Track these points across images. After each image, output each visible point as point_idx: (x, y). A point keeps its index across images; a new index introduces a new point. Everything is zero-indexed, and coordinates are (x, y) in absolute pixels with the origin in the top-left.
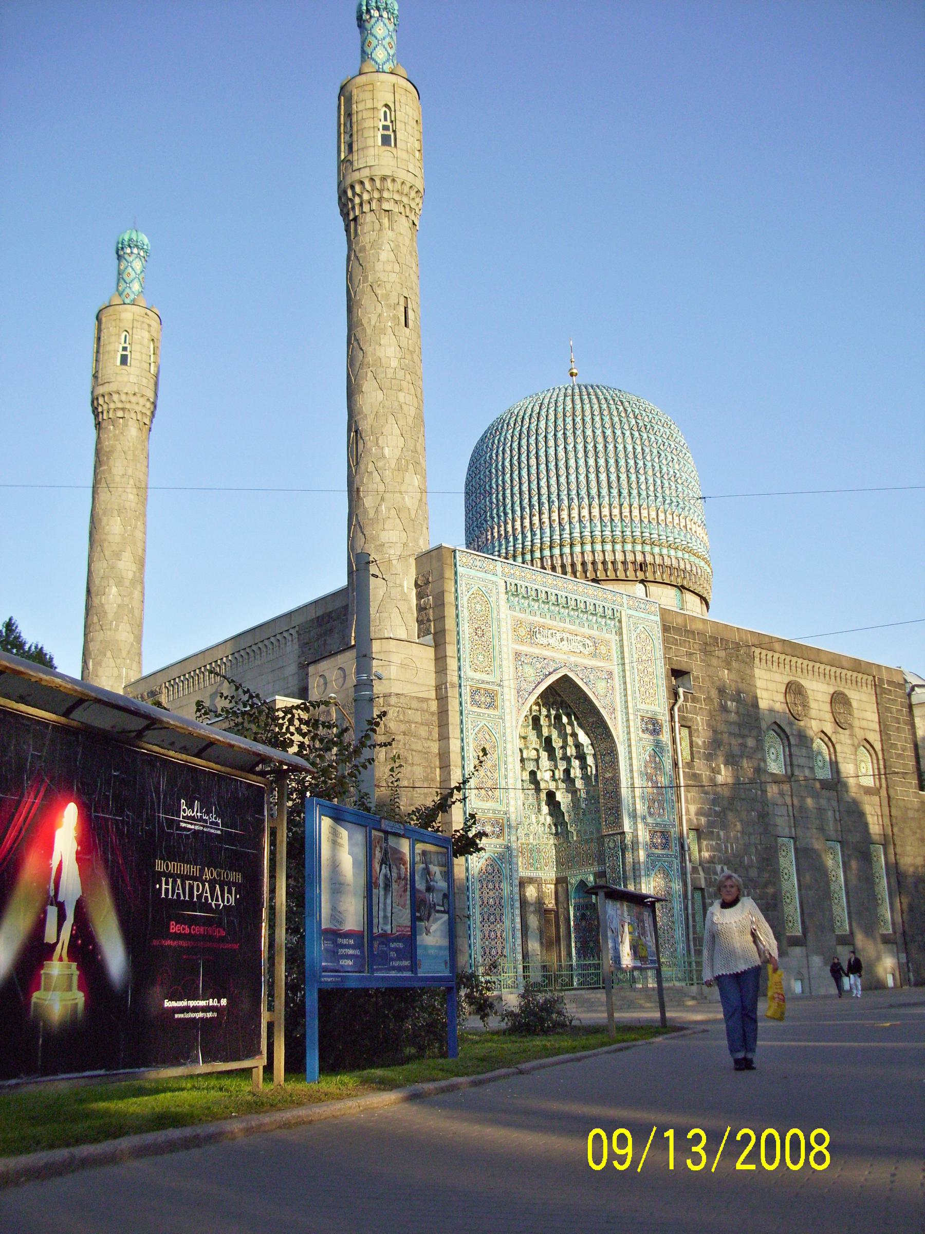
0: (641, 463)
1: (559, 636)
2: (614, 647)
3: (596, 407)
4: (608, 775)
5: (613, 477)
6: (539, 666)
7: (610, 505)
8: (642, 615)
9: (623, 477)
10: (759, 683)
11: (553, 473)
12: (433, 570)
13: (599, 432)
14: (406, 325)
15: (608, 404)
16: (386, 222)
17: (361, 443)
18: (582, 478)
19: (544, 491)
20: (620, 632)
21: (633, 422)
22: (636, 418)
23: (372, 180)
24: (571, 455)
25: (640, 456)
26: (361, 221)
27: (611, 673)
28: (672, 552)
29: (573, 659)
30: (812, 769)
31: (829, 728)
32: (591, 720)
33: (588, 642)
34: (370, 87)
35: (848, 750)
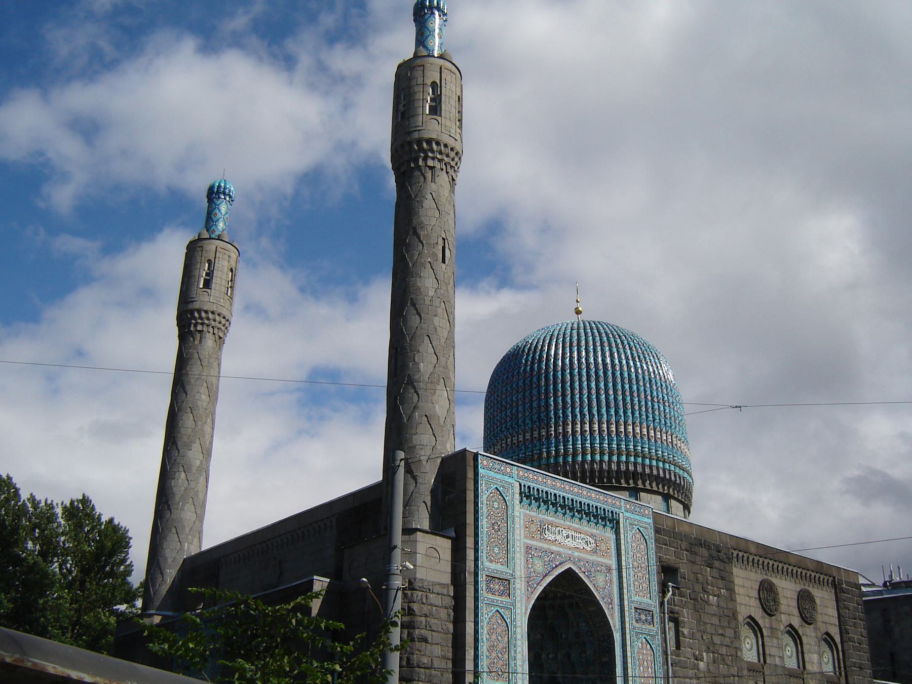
0: (635, 388)
3: (598, 339)
4: (605, 659)
10: (737, 581)
12: (456, 473)
14: (444, 261)
20: (617, 533)
29: (576, 554)
30: (782, 658)
31: (796, 622)
35: (813, 642)
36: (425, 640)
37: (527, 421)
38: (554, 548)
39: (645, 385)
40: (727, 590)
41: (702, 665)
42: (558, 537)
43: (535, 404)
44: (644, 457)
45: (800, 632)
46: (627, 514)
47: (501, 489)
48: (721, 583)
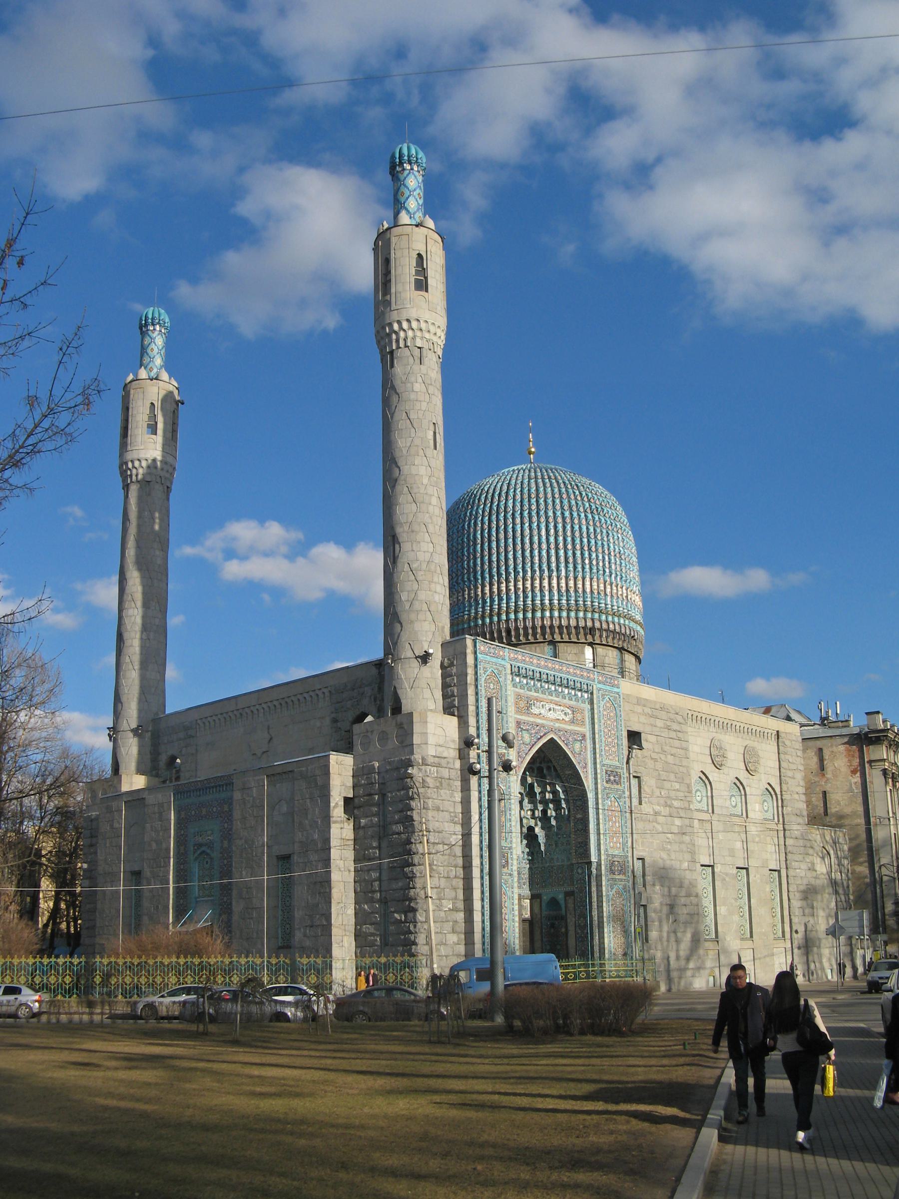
1: (547, 706)
2: (587, 715)
3: (556, 490)
4: (579, 816)
5: (570, 553)
6: (533, 732)
8: (608, 688)
9: (578, 553)
11: (519, 547)
13: (559, 513)
14: (435, 448)
15: (566, 488)
17: (397, 546)
18: (544, 553)
19: (511, 562)
20: (591, 702)
21: (587, 505)
22: (589, 501)
24: (535, 532)
25: (592, 536)
26: (398, 354)
27: (584, 736)
28: (616, 619)
29: (557, 725)
32: (567, 772)
33: (568, 711)
38: (539, 721)
46: (600, 686)
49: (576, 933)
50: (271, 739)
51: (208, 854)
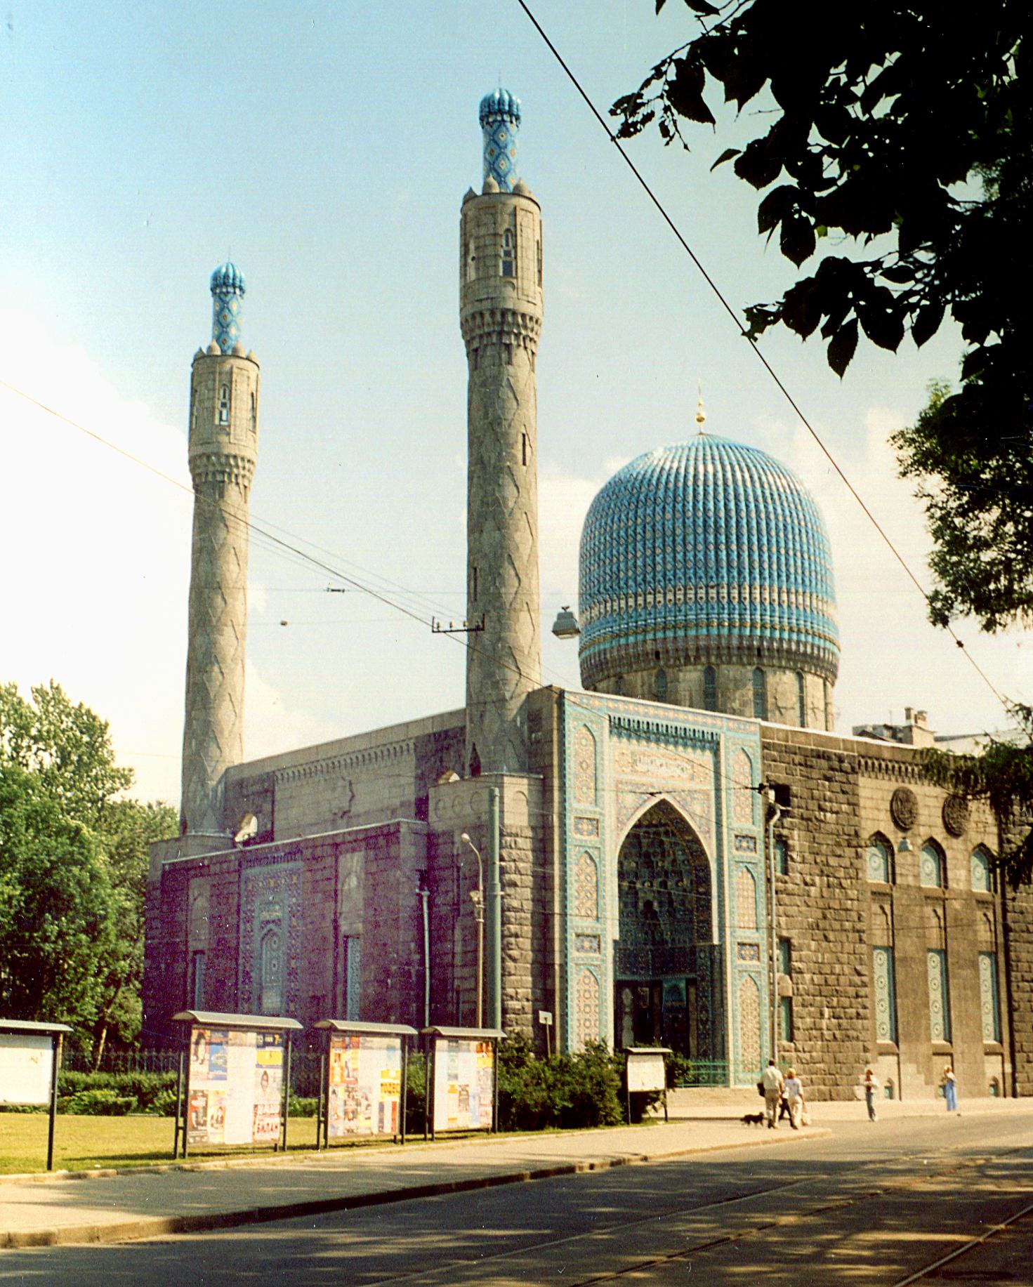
7: (729, 585)
10: (863, 792)
12: (545, 710)
14: (524, 464)
16: (504, 356)
23: (493, 313)
30: (917, 876)
31: (940, 835)
33: (685, 765)
34: (492, 211)
36: (515, 885)
37: (631, 582)
39: (777, 535)
40: (849, 804)
41: (813, 889)
42: (651, 768)
43: (639, 563)
44: (773, 628)
45: (944, 846)
47: (589, 725)
48: (841, 797)
49: (698, 1029)
50: (353, 797)
51: (275, 934)
